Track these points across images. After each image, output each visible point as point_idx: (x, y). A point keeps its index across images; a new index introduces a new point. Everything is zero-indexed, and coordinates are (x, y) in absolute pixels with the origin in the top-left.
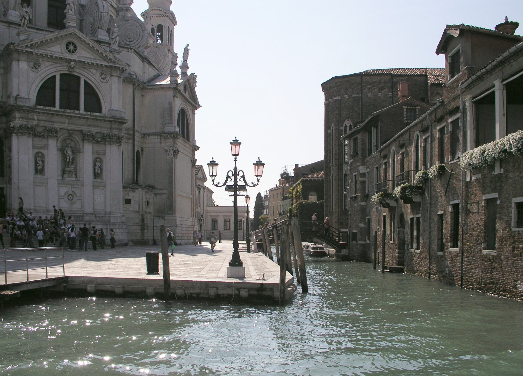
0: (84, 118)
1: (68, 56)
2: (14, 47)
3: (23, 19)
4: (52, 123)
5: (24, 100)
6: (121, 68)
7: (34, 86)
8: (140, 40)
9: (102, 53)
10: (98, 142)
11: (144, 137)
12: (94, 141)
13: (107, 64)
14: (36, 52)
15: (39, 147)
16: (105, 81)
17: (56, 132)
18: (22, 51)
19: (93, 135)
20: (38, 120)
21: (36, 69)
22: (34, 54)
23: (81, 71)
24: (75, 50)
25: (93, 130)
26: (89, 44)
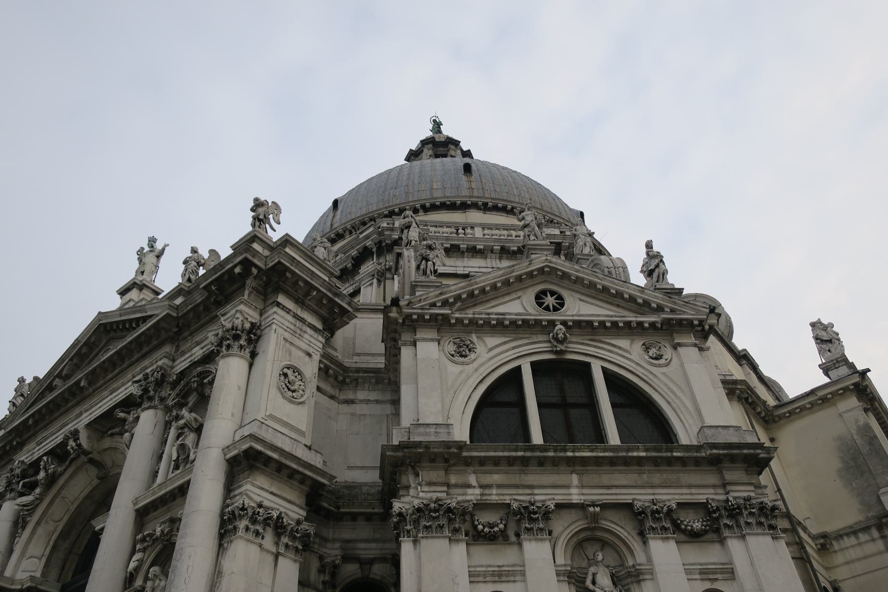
2: (400, 312)
3: (424, 261)
4: (528, 491)
5: (432, 430)
7: (462, 397)
10: (694, 536)
12: (682, 537)
13: (652, 319)
14: (457, 315)
15: (493, 574)
16: (662, 361)
18: (421, 316)
20: (481, 487)
21: (465, 356)
24: (562, 305)
25: (669, 497)
26: (592, 285)
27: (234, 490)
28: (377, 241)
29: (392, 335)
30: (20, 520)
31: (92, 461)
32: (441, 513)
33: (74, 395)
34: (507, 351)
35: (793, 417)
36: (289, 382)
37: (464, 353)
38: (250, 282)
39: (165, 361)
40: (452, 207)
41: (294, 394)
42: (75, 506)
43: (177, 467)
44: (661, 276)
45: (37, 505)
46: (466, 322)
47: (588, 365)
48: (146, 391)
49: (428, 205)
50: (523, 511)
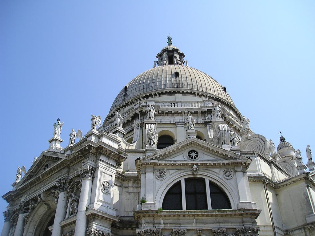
0: (212, 215)
1: (191, 162)
4: (179, 225)
6: (243, 163)
8: (263, 149)
9: (222, 154)
11: (287, 234)
14: (160, 163)
16: (230, 177)
17: (184, 233)
19: (223, 232)
20: (164, 223)
21: (163, 177)
22: (158, 165)
23: (204, 173)
24: (197, 156)
26: (208, 149)
27: (89, 225)
28: (140, 111)
29: (139, 169)
30: (25, 221)
31: (45, 204)
32: (151, 233)
33: (38, 181)
34: (177, 175)
35: (284, 187)
36: (105, 187)
37: (162, 176)
38: (91, 151)
39: (66, 175)
40: (170, 93)
41: (107, 191)
42: (41, 217)
43: (72, 214)
44: (234, 143)
45: (30, 216)
46: (163, 165)
47: (204, 179)
48: (60, 186)
49: (160, 93)
50: (176, 232)
